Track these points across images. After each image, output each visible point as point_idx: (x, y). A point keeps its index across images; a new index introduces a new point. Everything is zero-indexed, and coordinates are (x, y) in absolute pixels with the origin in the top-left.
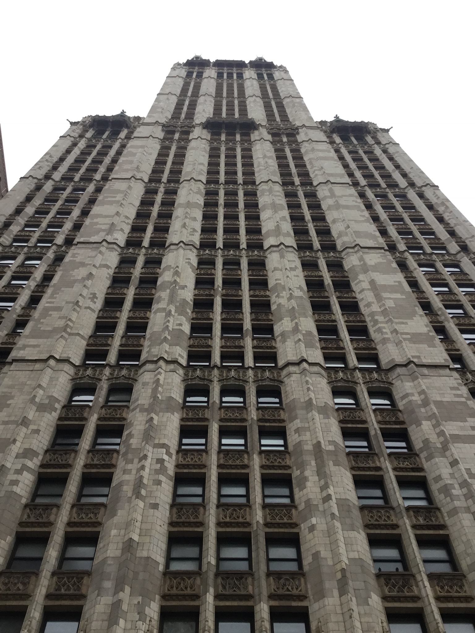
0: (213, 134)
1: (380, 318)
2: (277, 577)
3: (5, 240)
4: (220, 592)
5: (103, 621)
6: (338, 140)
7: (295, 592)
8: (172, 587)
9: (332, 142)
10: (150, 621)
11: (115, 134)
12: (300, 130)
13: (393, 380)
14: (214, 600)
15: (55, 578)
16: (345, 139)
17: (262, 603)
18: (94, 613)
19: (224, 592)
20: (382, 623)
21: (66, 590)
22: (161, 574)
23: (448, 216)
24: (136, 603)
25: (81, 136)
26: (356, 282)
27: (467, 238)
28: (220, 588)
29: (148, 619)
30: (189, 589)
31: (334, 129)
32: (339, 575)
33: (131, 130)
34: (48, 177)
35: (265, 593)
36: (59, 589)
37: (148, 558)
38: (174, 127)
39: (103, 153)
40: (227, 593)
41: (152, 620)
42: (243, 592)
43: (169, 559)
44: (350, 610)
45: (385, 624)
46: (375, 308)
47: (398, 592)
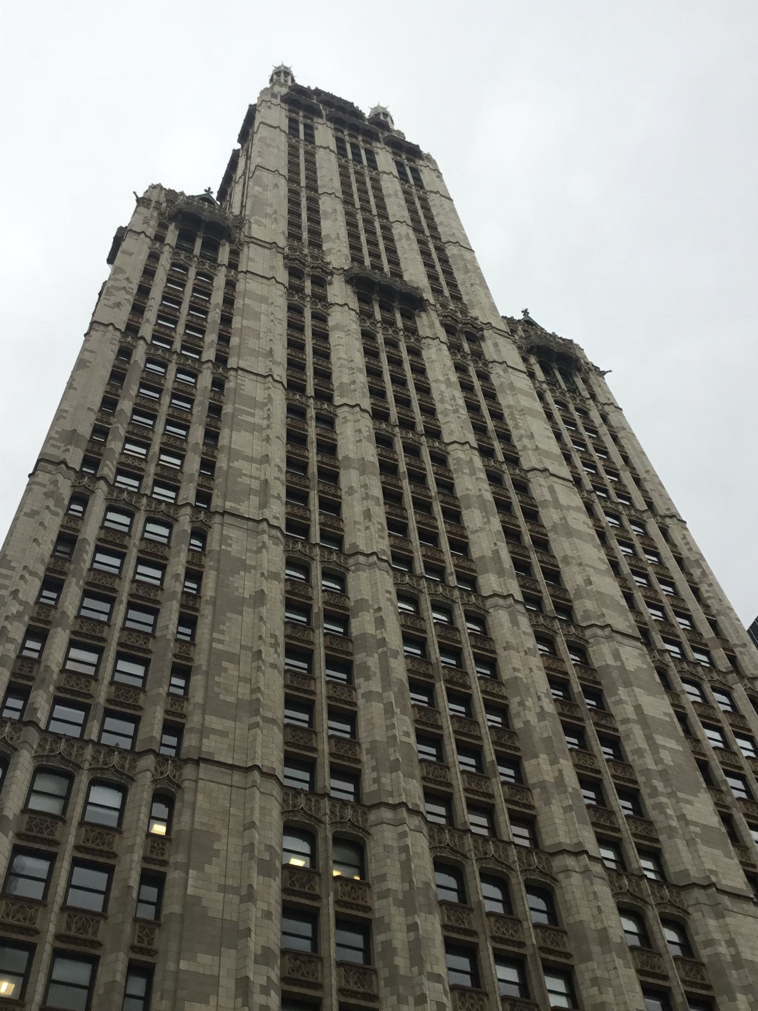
0: (361, 299)
1: (658, 784)
3: (109, 473)
6: (540, 375)
9: (532, 375)
11: (211, 247)
12: (486, 333)
13: (688, 906)
16: (546, 370)
23: (707, 592)
25: (159, 238)
26: (613, 699)
27: (736, 646)
31: (532, 347)
33: (235, 247)
34: (132, 329)
38: (301, 263)
39: (203, 290)
46: (649, 762)
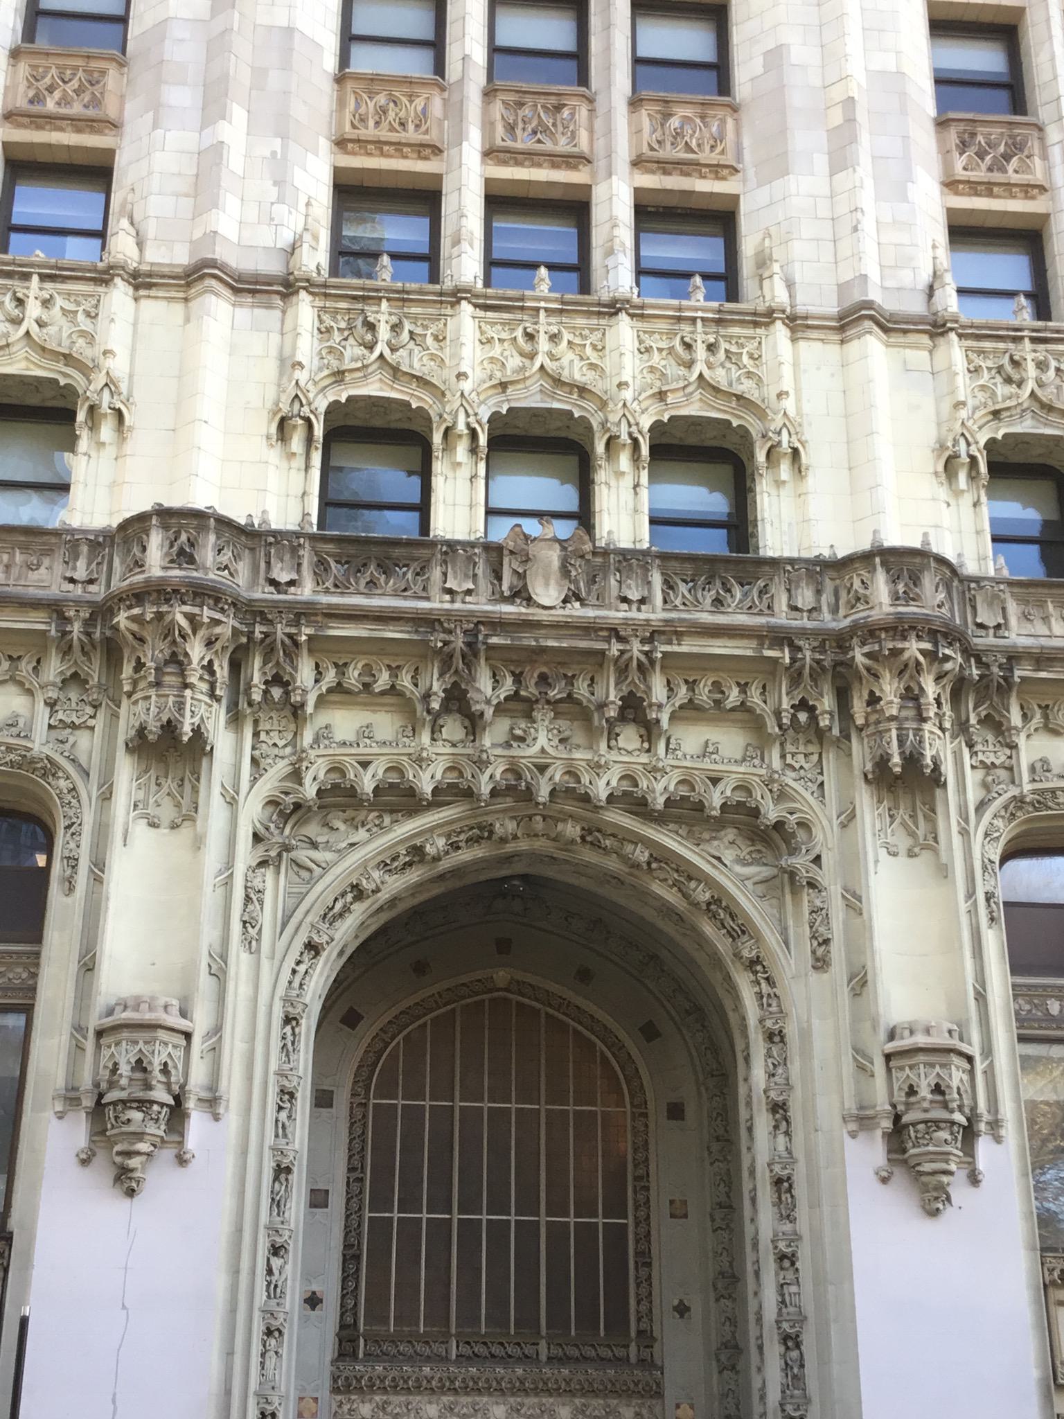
2: (658, 112)
4: (499, 142)
5: (177, 195)
7: (706, 156)
8: (363, 120)
10: (308, 204)
14: (483, 162)
15: (23, 68)
17: (614, 178)
18: (150, 173)
19: (509, 143)
20: (934, 247)
21: (58, 104)
22: (331, 79)
24: (268, 154)
28: (500, 130)
29: (303, 200)
30: (411, 127)
32: (837, 117)
35: (623, 151)
36: (37, 99)
37: (289, 31)
40: (519, 145)
41: (313, 201)
42: (562, 145)
43: (349, 38)
44: (856, 210)
45: (943, 253)
47: (990, 169)
